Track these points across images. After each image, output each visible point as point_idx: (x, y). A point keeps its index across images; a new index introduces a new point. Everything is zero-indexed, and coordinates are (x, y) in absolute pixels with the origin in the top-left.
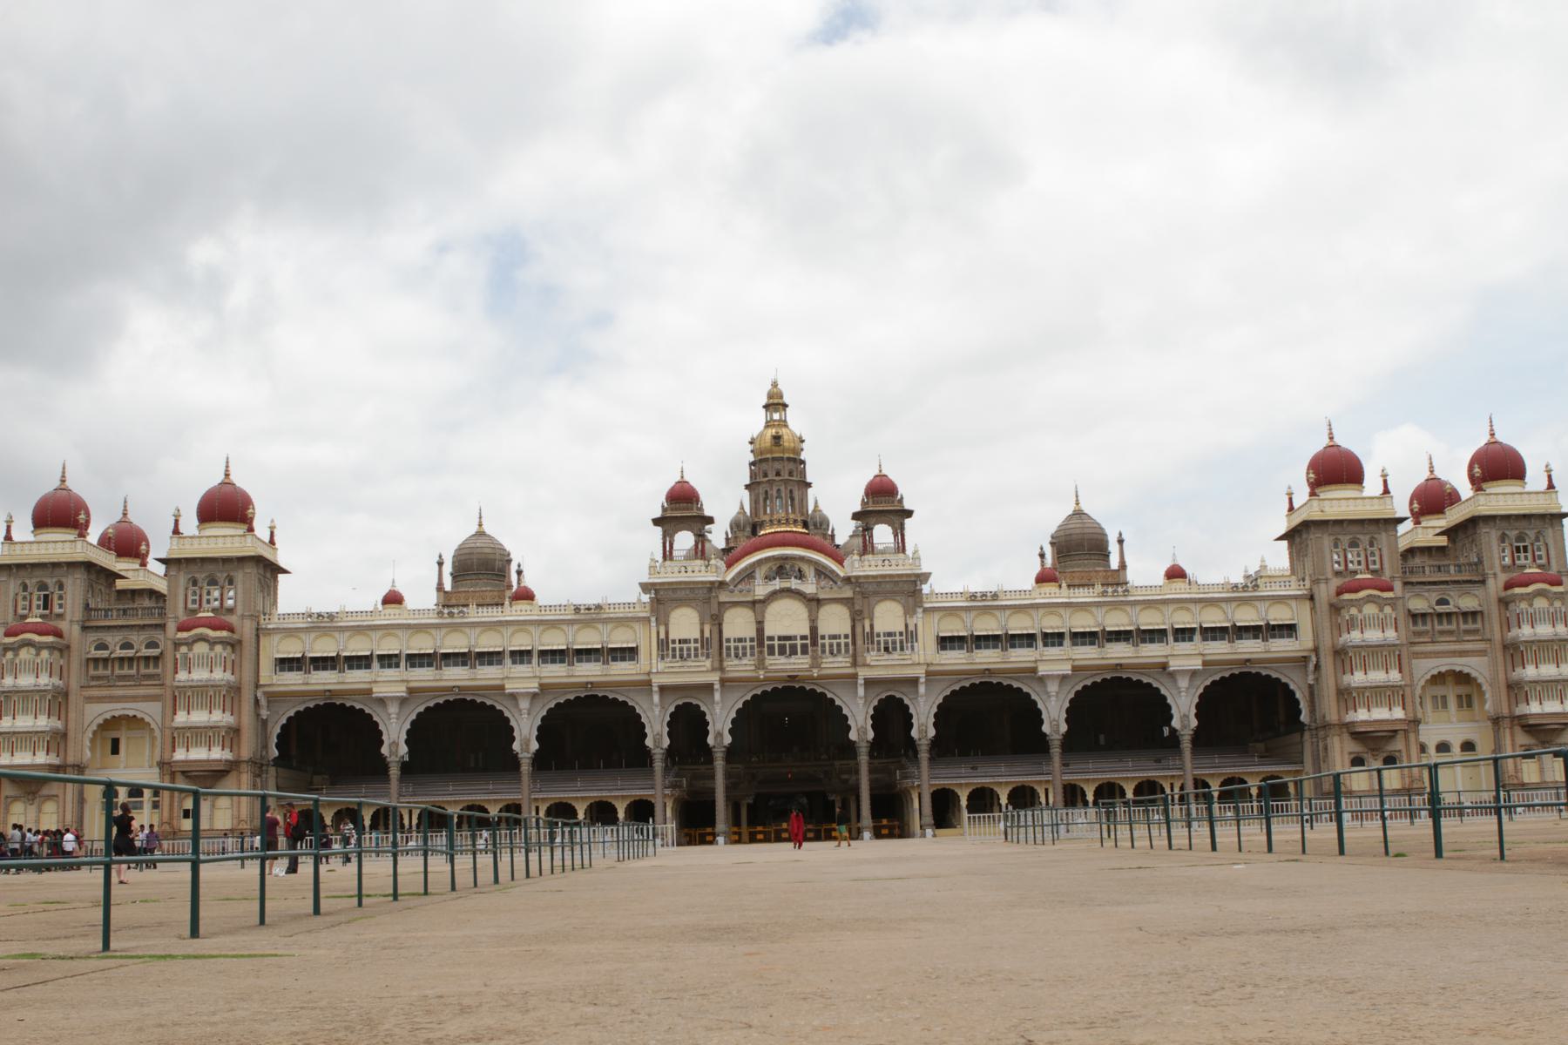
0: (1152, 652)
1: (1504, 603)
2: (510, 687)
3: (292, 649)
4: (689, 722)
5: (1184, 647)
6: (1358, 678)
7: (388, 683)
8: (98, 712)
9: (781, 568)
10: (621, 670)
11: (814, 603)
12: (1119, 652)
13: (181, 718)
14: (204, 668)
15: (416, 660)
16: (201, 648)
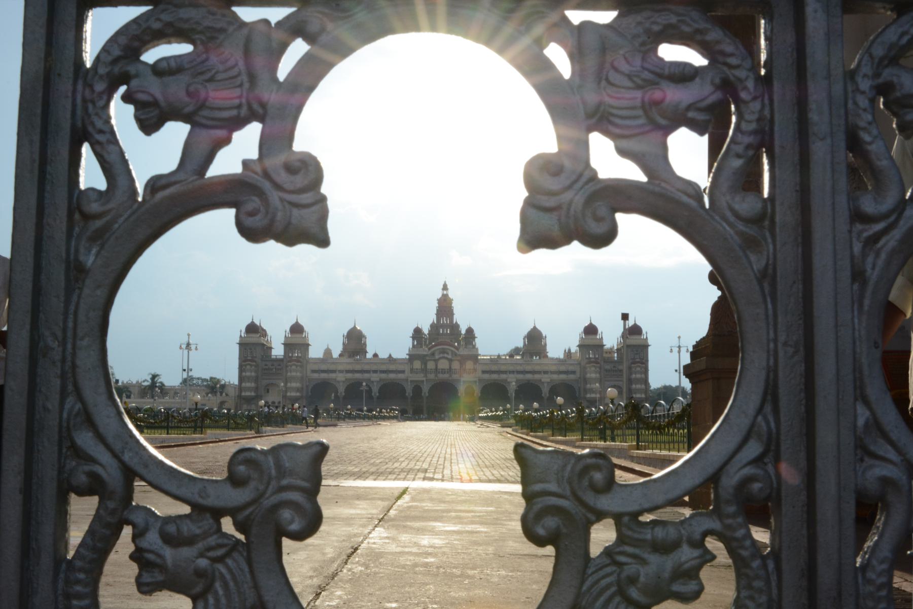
0: (537, 376)
1: (630, 368)
2: (372, 379)
3: (316, 367)
4: (417, 389)
5: (546, 376)
6: (588, 386)
7: (341, 377)
8: (265, 382)
9: (443, 351)
10: (401, 376)
11: (450, 361)
12: (529, 376)
13: (289, 385)
14: (295, 373)
15: (348, 371)
16: (294, 367)
